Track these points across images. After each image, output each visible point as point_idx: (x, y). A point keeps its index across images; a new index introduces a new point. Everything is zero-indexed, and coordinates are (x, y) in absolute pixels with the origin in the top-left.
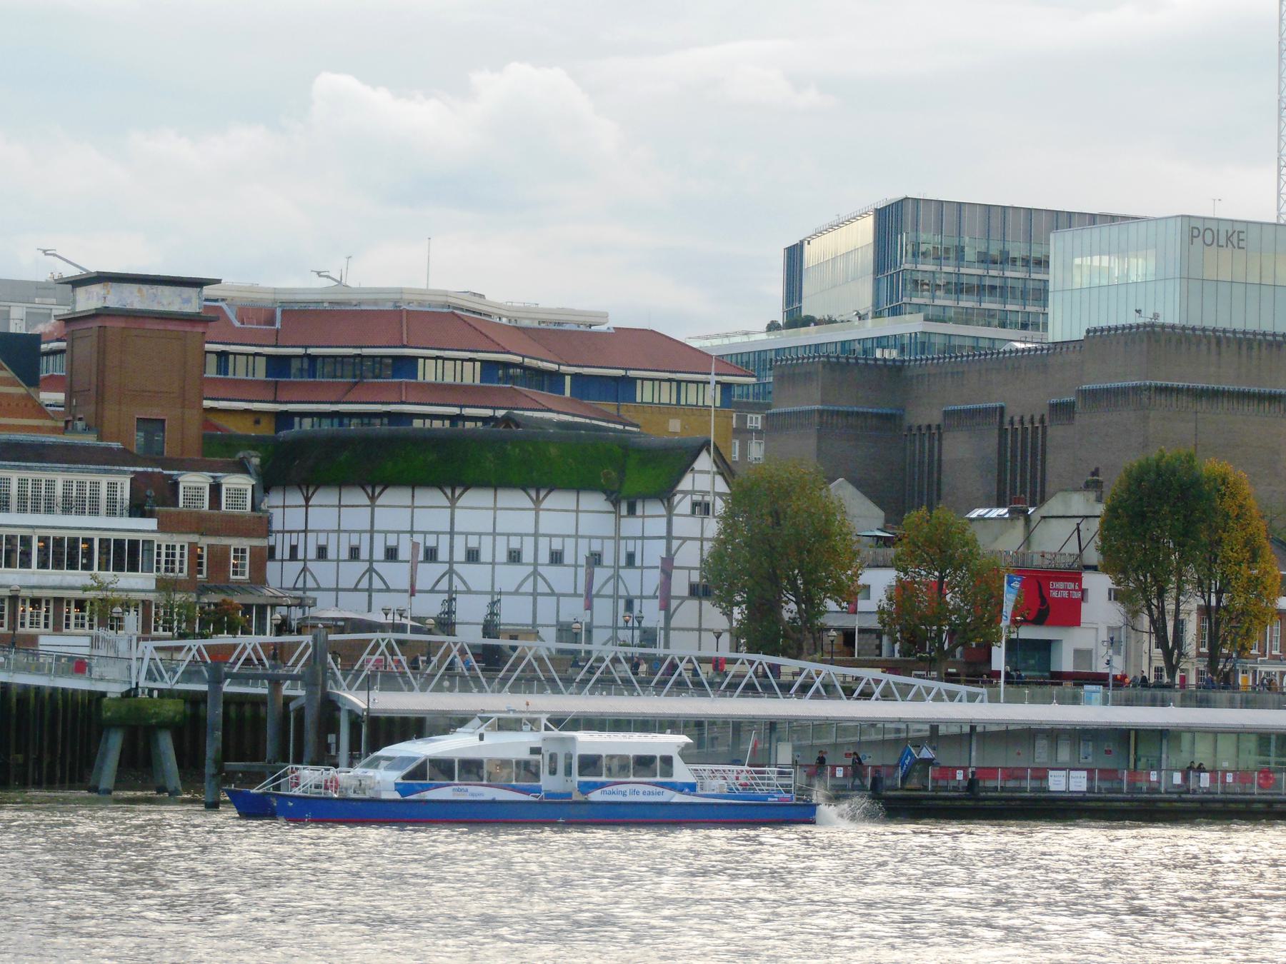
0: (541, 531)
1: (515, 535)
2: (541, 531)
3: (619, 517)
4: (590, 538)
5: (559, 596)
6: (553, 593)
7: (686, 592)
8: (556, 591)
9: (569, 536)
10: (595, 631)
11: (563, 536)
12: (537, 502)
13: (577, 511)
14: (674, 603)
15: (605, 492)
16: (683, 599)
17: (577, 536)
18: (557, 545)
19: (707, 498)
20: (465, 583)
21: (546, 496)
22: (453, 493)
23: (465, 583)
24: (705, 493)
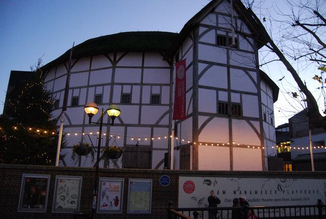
0: (116, 81)
1: (99, 85)
2: (116, 81)
3: (171, 68)
4: (152, 85)
5: (127, 126)
6: (122, 124)
7: (214, 110)
8: (125, 122)
9: (136, 84)
10: (154, 152)
11: (132, 84)
12: (114, 63)
13: (143, 67)
14: (201, 120)
15: (162, 55)
16: (211, 116)
17: (142, 84)
18: (127, 90)
19: (230, 35)
20: (69, 120)
21: (120, 59)
22: (70, 65)
23: (69, 120)
24: (228, 31)
